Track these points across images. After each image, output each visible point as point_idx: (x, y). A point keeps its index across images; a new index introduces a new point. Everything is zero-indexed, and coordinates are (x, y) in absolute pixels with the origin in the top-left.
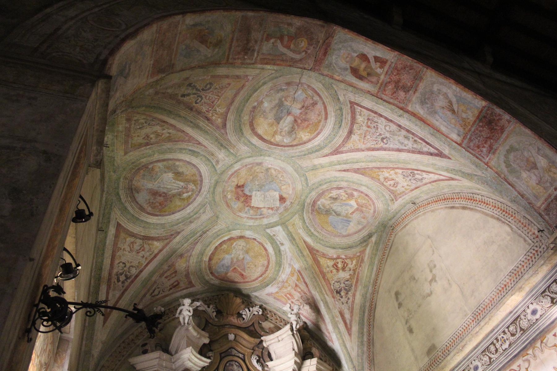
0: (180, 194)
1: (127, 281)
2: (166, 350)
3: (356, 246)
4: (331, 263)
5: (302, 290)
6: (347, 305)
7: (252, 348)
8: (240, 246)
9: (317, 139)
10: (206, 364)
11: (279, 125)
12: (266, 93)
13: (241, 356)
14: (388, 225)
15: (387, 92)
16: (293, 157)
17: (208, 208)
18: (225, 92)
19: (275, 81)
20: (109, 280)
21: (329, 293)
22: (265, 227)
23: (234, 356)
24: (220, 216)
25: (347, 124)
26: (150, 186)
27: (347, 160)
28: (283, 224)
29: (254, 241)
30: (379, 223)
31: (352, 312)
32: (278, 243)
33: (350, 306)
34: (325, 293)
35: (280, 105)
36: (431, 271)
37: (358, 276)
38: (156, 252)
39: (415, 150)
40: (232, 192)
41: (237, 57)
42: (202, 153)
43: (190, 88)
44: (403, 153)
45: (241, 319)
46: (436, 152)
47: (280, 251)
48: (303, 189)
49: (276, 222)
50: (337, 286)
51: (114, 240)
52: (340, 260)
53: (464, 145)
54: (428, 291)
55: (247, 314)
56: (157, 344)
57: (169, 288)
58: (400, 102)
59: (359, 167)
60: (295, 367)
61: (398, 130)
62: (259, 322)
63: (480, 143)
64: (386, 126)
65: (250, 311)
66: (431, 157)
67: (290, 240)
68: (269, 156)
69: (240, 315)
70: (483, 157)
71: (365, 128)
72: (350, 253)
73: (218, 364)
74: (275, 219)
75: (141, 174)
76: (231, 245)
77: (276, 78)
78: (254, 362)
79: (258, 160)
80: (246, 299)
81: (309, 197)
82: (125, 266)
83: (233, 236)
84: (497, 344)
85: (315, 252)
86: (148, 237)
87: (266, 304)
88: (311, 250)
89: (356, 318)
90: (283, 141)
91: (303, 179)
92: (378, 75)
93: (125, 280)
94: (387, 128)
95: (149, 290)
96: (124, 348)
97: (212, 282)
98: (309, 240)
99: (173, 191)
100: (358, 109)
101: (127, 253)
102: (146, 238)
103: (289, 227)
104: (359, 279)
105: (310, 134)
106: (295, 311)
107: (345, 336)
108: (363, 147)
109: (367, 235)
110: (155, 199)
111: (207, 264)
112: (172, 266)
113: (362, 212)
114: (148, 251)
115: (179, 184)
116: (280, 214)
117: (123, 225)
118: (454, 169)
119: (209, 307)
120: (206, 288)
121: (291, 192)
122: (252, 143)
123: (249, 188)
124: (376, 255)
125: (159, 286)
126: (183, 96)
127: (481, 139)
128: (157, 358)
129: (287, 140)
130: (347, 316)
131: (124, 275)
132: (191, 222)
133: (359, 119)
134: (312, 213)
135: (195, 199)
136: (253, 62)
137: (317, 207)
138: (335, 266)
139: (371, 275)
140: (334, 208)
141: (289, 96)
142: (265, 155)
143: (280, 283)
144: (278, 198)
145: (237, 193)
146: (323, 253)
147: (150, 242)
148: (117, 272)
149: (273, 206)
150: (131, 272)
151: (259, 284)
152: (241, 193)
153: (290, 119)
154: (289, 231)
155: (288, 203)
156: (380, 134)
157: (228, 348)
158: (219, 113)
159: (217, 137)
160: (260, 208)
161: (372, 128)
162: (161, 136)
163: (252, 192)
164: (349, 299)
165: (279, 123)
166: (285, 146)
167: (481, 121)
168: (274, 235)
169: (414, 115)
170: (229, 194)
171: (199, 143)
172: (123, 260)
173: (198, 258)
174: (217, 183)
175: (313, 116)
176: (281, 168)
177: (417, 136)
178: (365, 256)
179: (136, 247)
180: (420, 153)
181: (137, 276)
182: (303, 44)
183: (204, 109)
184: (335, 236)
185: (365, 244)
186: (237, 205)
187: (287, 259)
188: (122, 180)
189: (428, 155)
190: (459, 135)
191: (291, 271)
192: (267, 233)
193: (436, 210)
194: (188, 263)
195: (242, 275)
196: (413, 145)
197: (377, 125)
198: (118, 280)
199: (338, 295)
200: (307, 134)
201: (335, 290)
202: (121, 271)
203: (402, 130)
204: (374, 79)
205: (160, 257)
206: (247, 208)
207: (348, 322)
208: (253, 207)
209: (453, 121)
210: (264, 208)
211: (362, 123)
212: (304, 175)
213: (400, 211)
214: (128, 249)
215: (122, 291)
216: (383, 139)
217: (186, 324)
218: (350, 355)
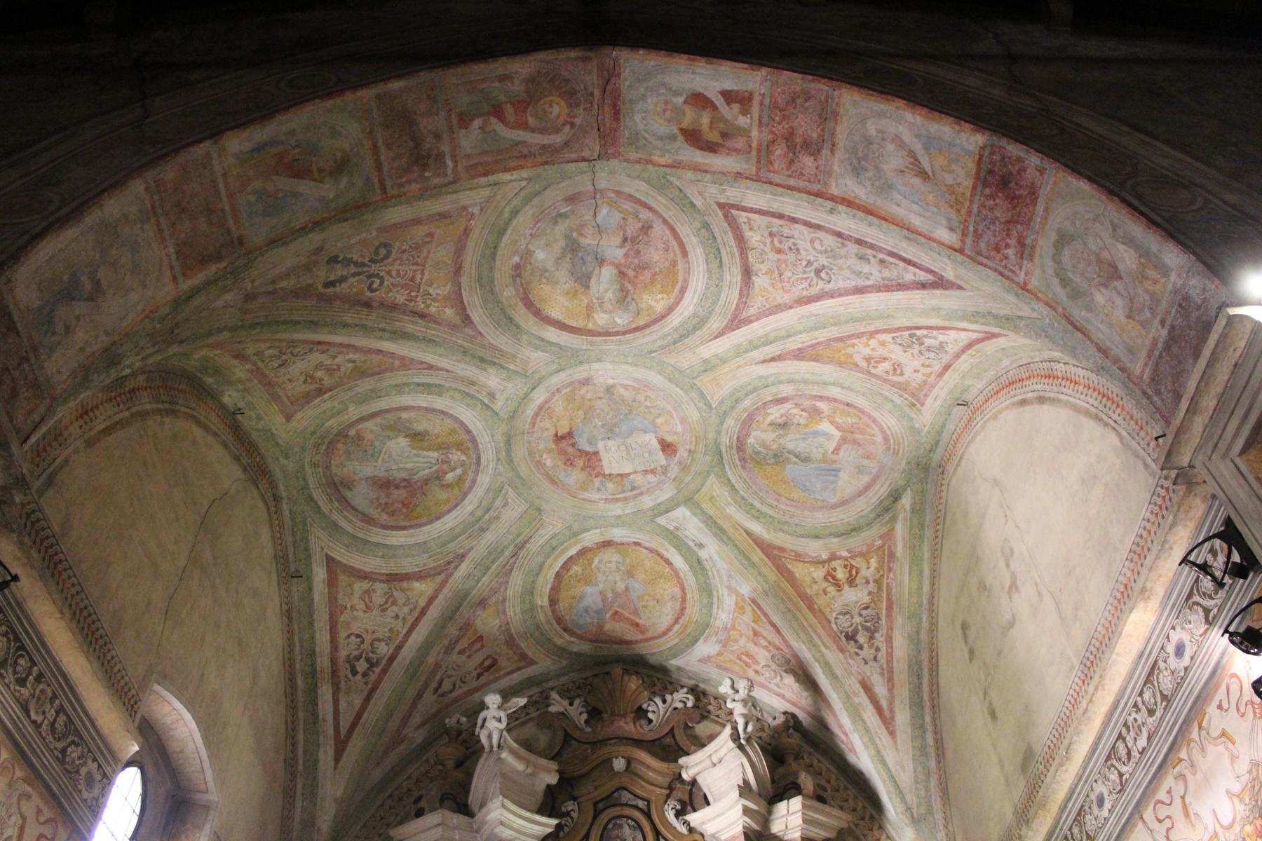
0: (438, 477)
1: (373, 672)
2: (464, 809)
3: (869, 524)
4: (819, 573)
5: (769, 643)
6: (875, 664)
7: (666, 785)
8: (610, 562)
9: (685, 301)
10: (549, 830)
11: (591, 292)
12: (528, 232)
13: (641, 804)
14: (933, 465)
15: (776, 165)
16: (651, 352)
17: (511, 494)
18: (429, 252)
19: (536, 201)
20: (334, 673)
21: (829, 642)
22: (650, 513)
23: (627, 805)
24: (544, 506)
25: (733, 255)
26: (368, 470)
27: (766, 335)
28: (689, 500)
29: (638, 548)
30: (908, 463)
31: (890, 680)
32: (692, 544)
33: (885, 666)
34: (819, 643)
35: (573, 247)
36: (1008, 566)
37: (889, 594)
38: (422, 603)
39: (890, 283)
40: (550, 451)
41: (404, 180)
42: (447, 385)
43: (339, 266)
44: (868, 295)
45: (643, 722)
46: (930, 277)
47: (699, 561)
48: (702, 416)
49: (671, 499)
50: (844, 622)
51: (329, 593)
52: (839, 562)
53: (967, 252)
54: (1008, 616)
55: (657, 710)
56: (447, 794)
57: (475, 673)
58: (809, 181)
59: (800, 346)
60: (748, 820)
61: (840, 245)
62: (686, 726)
63: (999, 238)
64: (812, 241)
65: (664, 701)
66: (925, 292)
67: (715, 535)
68: (599, 360)
69: (641, 713)
70: (1013, 272)
71: (772, 256)
72: (857, 542)
73: (587, 827)
74: (667, 493)
75: (341, 452)
76: (590, 564)
77: (537, 194)
78: (670, 815)
79: (579, 373)
80: (660, 676)
81: (723, 433)
82: (363, 642)
83: (587, 544)
84: (1128, 739)
85: (776, 552)
86: (396, 574)
87: (704, 681)
88: (766, 548)
89: (903, 693)
90: (615, 322)
91: (693, 395)
92: (746, 132)
93: (369, 669)
94: (817, 244)
95: (426, 685)
97: (575, 649)
98: (756, 527)
99: (422, 473)
100: (742, 217)
101: (361, 614)
102: (394, 578)
103: (704, 506)
104: (894, 599)
105: (665, 296)
106: (743, 693)
107: (880, 739)
108: (787, 298)
109: (888, 496)
110: (388, 496)
111: (549, 613)
112: (466, 627)
113: (856, 443)
114: (404, 605)
115: (428, 457)
116: (674, 480)
117: (339, 558)
118: (978, 313)
119: (571, 704)
120: (564, 662)
121: (679, 429)
122: (548, 342)
123: (586, 435)
124: (921, 538)
125: (449, 673)
126: (328, 285)
127: (997, 227)
128: (439, 825)
129: (622, 320)
130: (881, 690)
131: (362, 660)
132: (483, 530)
133: (753, 238)
134: (743, 467)
135: (474, 481)
136: (450, 178)
137: (749, 451)
138: (830, 576)
139: (920, 588)
140: (791, 446)
141: (585, 225)
142: (589, 361)
143: (720, 633)
144: (658, 446)
145: (563, 452)
146: (796, 552)
147: (405, 584)
148: (348, 656)
149: (653, 466)
150: (378, 651)
151: (677, 640)
152: (570, 450)
153: (607, 272)
154: (706, 514)
155: (682, 453)
156: (809, 263)
157: (613, 789)
158: (439, 298)
159: (461, 346)
160: (628, 475)
161: (787, 251)
162: (339, 369)
163: (596, 445)
165: (588, 287)
166: (624, 333)
167: (986, 184)
168: (677, 528)
169: (849, 203)
170: (544, 456)
171: (431, 367)
172: (355, 628)
173: (523, 602)
174: (509, 441)
175: (655, 255)
176: (635, 380)
177: (881, 250)
178: (895, 545)
179: (378, 599)
180: (902, 287)
181: (392, 659)
182: (556, 110)
183: (400, 299)
184: (813, 509)
185: (887, 517)
186: (573, 477)
187: (720, 577)
188: (308, 470)
189: (918, 289)
190: (952, 229)
191: (737, 603)
192: (660, 526)
193: (1000, 412)
194: (503, 617)
195: (637, 625)
196: (880, 272)
197: (795, 244)
198: (354, 673)
199: (852, 642)
200: (660, 296)
201: (841, 632)
202: (355, 653)
203: (848, 243)
204: (740, 143)
205: (433, 613)
206: (597, 481)
207: (884, 703)
208: (610, 475)
209: (931, 197)
210: (635, 472)
211: (762, 246)
212: (693, 386)
213: (943, 426)
214: (361, 606)
215: (366, 693)
216: (818, 272)
217: (495, 749)
218: (895, 781)
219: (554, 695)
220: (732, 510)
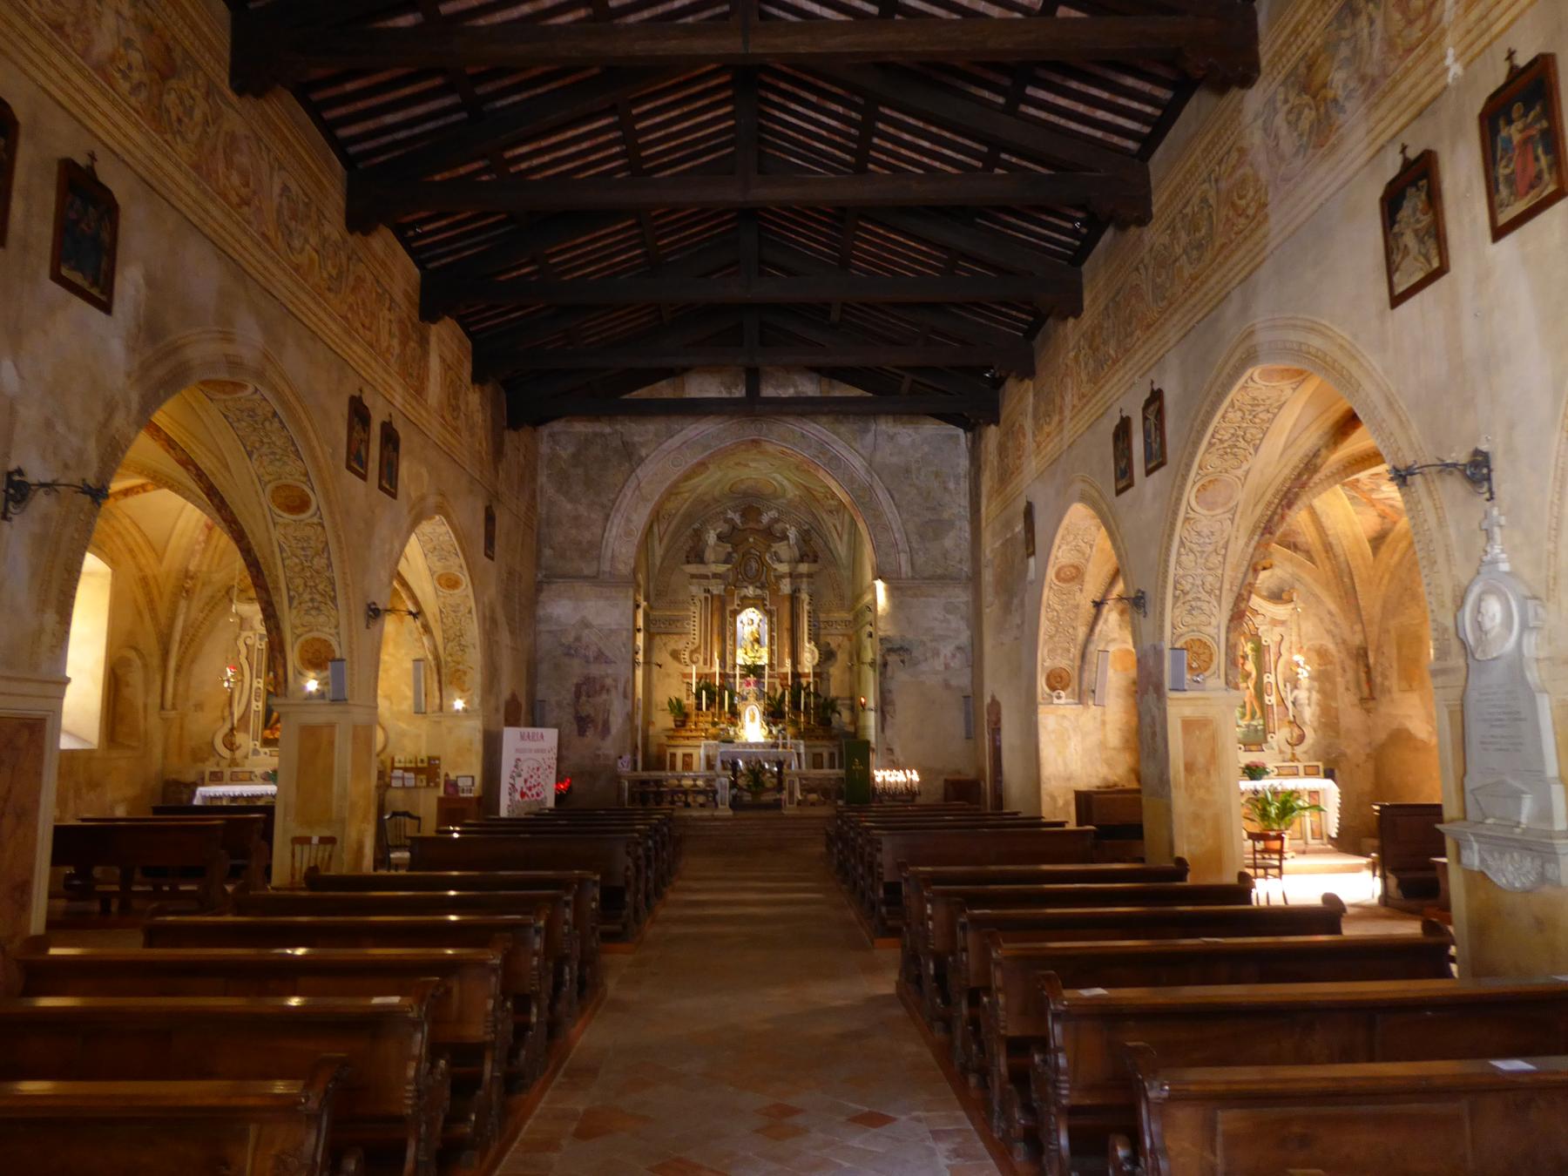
31: (843, 526)
88: (805, 487)
130: (839, 528)
181: (676, 513)
205: (691, 500)
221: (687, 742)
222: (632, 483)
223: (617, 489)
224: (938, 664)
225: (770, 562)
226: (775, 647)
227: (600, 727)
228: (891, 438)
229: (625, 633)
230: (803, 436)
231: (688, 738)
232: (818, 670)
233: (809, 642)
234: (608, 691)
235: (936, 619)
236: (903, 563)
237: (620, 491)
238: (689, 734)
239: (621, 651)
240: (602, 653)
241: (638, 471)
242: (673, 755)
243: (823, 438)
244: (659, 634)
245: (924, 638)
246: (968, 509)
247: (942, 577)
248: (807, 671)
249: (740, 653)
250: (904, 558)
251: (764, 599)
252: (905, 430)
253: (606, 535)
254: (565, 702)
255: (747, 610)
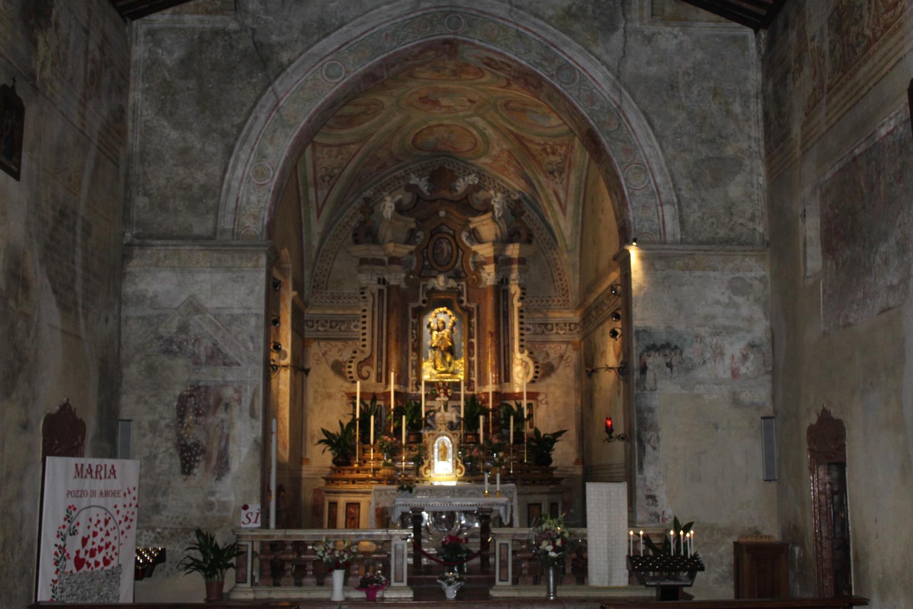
4: (539, 148)
13: (451, 232)
38: (354, 152)
47: (484, 134)
50: (549, 167)
88: (516, 136)
96: (341, 231)
98: (512, 128)
102: (340, 145)
130: (562, 195)
164: (563, 180)
181: (340, 174)
198: (324, 181)
205: (359, 156)
207: (563, 201)
219: (412, 175)
220: (501, 121)
221: (352, 487)
222: (268, 100)
223: (245, 110)
224: (723, 370)
225: (468, 244)
226: (475, 358)
227: (214, 463)
228: (649, 39)
229: (253, 321)
230: (519, 35)
231: (354, 481)
232: (533, 390)
233: (522, 352)
234: (227, 406)
235: (718, 302)
236: (668, 219)
237: (249, 113)
238: (355, 475)
239: (247, 348)
240: (219, 350)
241: (277, 82)
242: (333, 505)
243: (549, 38)
244: (315, 339)
245: (702, 331)
246: (762, 143)
247: (727, 241)
248: (517, 390)
249: (427, 366)
250: (669, 212)
251: (460, 293)
252: (668, 29)
253: (228, 176)
254: (163, 423)
255: (437, 311)
